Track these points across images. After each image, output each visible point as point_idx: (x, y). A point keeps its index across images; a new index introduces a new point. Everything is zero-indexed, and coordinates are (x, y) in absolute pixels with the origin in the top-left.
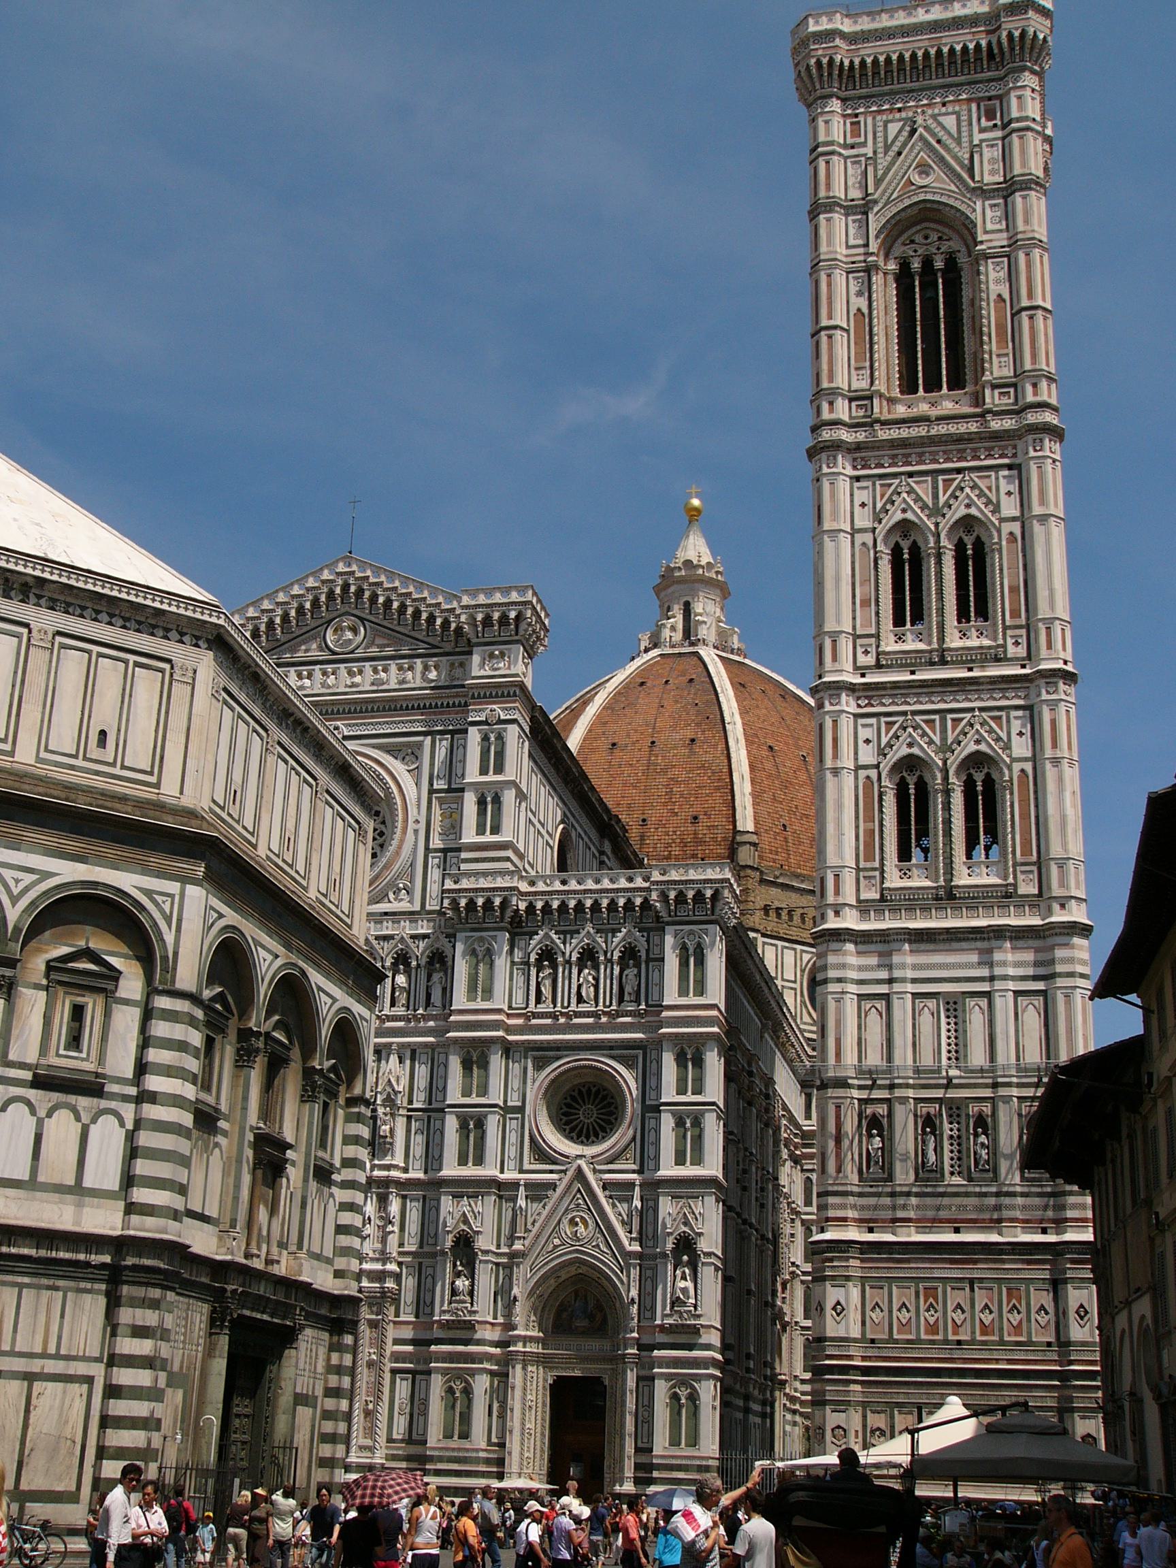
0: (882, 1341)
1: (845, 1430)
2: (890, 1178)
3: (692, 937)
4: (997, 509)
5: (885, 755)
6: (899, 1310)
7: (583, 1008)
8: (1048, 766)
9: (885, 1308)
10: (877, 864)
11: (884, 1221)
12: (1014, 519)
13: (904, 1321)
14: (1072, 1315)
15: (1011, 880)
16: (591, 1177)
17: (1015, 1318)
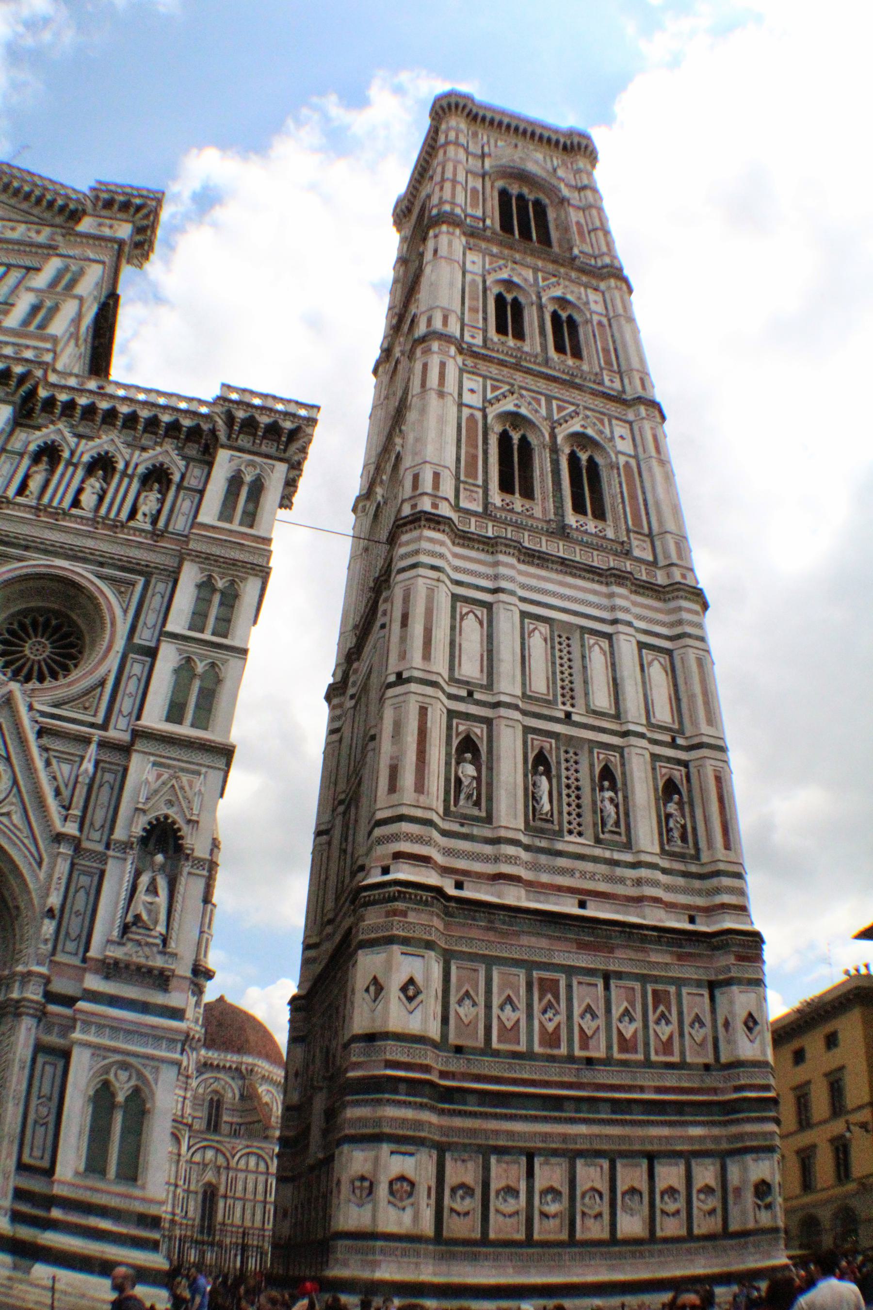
0: (474, 1051)
1: (412, 1184)
2: (489, 819)
3: (250, 469)
4: (587, 303)
5: (492, 404)
6: (502, 1008)
7: (74, 511)
8: (654, 463)
9: (481, 1000)
10: (480, 482)
11: (479, 876)
12: (601, 314)
13: (509, 1025)
14: (739, 1025)
15: (625, 539)
16: (23, 710)
17: (665, 1031)
